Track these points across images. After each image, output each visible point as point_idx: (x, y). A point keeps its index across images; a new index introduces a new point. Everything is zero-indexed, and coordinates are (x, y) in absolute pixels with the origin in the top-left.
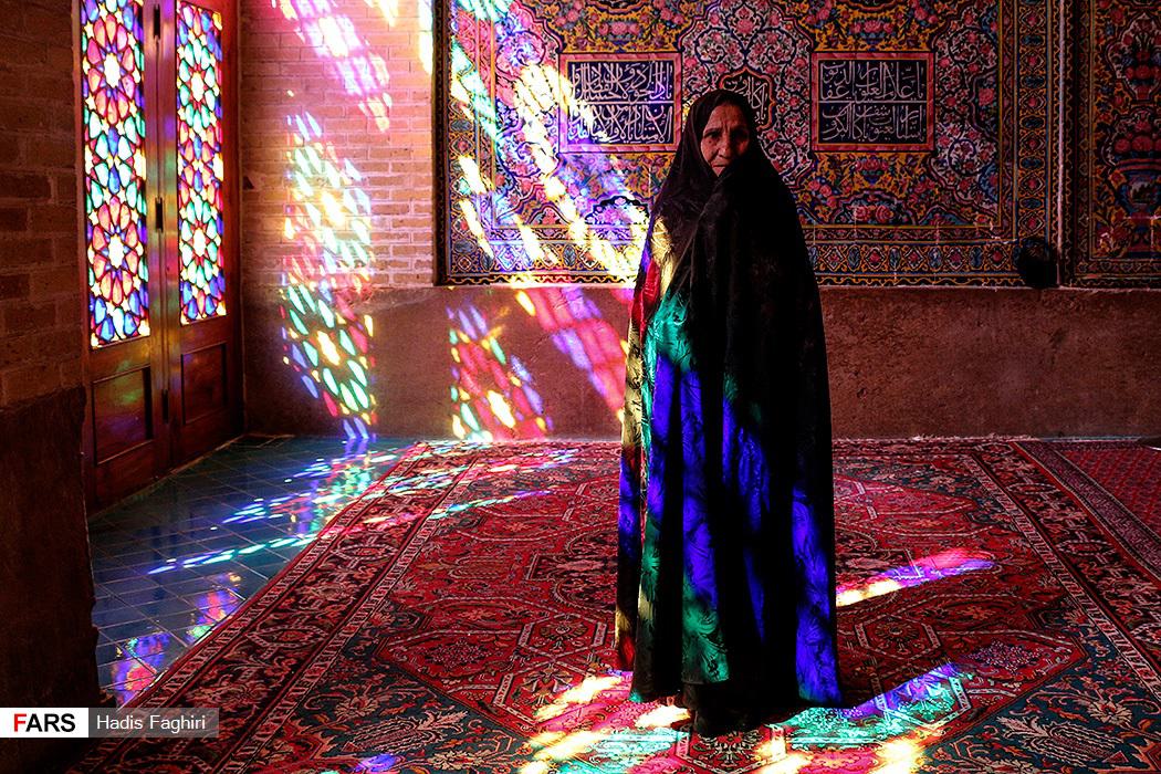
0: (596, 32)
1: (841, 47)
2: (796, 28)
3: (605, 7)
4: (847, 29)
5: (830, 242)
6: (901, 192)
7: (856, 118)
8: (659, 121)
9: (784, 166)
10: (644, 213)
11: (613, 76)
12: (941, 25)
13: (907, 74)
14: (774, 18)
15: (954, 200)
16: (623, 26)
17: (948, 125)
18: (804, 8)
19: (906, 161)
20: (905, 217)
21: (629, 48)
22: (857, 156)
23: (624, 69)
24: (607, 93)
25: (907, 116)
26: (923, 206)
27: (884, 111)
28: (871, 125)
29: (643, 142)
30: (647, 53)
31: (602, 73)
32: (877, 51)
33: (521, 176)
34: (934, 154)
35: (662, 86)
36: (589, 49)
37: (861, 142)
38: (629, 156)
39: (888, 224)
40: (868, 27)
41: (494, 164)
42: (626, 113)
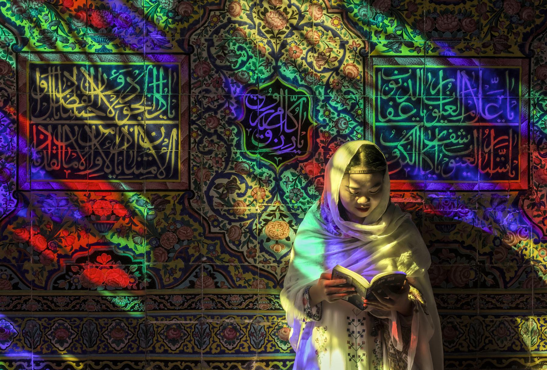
6: (484, 245)
7: (425, 146)
12: (538, 21)
23: (109, 75)
25: (493, 143)
27: (462, 137)
29: (137, 177)
35: (162, 101)
39: (467, 286)
40: (442, 23)
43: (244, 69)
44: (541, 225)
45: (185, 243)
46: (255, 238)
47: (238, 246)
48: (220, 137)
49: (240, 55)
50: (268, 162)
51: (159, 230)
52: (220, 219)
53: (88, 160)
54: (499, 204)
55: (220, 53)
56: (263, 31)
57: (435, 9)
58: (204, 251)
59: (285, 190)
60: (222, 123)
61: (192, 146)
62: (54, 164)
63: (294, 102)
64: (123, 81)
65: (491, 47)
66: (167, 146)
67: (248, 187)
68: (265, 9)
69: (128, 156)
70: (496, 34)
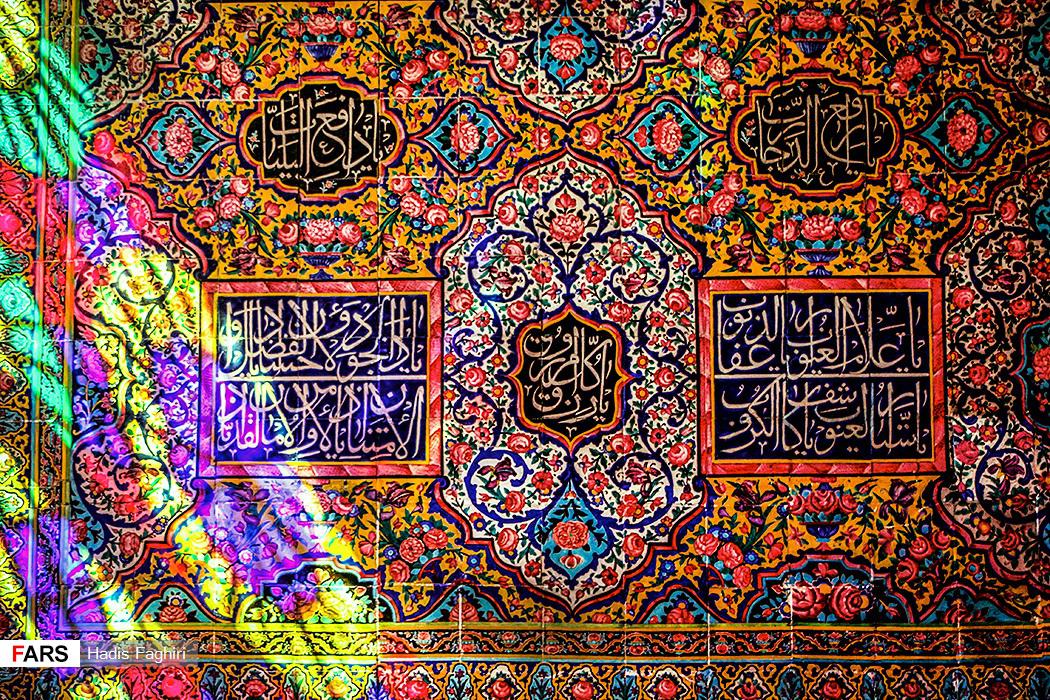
0: (275, 237)
1: (756, 269)
2: (669, 231)
3: (294, 190)
4: (769, 234)
5: (739, 659)
6: (882, 557)
7: (789, 408)
8: (396, 415)
9: (647, 506)
10: (365, 600)
11: (306, 325)
12: (953, 223)
13: (889, 320)
14: (624, 211)
15: (992, 573)
16: (327, 228)
17: (973, 420)
18: (684, 192)
19: (891, 493)
20: (890, 608)
21: (339, 270)
22: (791, 483)
23: (328, 310)
24: (293, 360)
25: (890, 404)
26: (928, 585)
27: (845, 394)
28: (819, 422)
29: (366, 457)
30: (375, 280)
31: (286, 319)
32: (829, 276)
33: (121, 523)
34: (948, 477)
35: (403, 346)
36: (260, 272)
37: (800, 457)
38: (337, 485)
39: (856, 620)
41: (66, 498)
42: (331, 400)
43: (521, 299)
44: (969, 526)
45: (435, 554)
46: (539, 547)
47: (512, 558)
48: (486, 399)
49: (515, 279)
50: (556, 435)
51: (398, 536)
52: (487, 519)
53: (297, 434)
54: (903, 494)
55: (487, 277)
56: (548, 244)
57: (800, 209)
58: (462, 564)
59: (582, 475)
60: (490, 377)
61: (446, 411)
62: (249, 439)
63: (594, 346)
64: (348, 319)
65: (885, 262)
66: (410, 412)
67: (527, 471)
68: (552, 213)
69: (354, 427)
70: (892, 243)
